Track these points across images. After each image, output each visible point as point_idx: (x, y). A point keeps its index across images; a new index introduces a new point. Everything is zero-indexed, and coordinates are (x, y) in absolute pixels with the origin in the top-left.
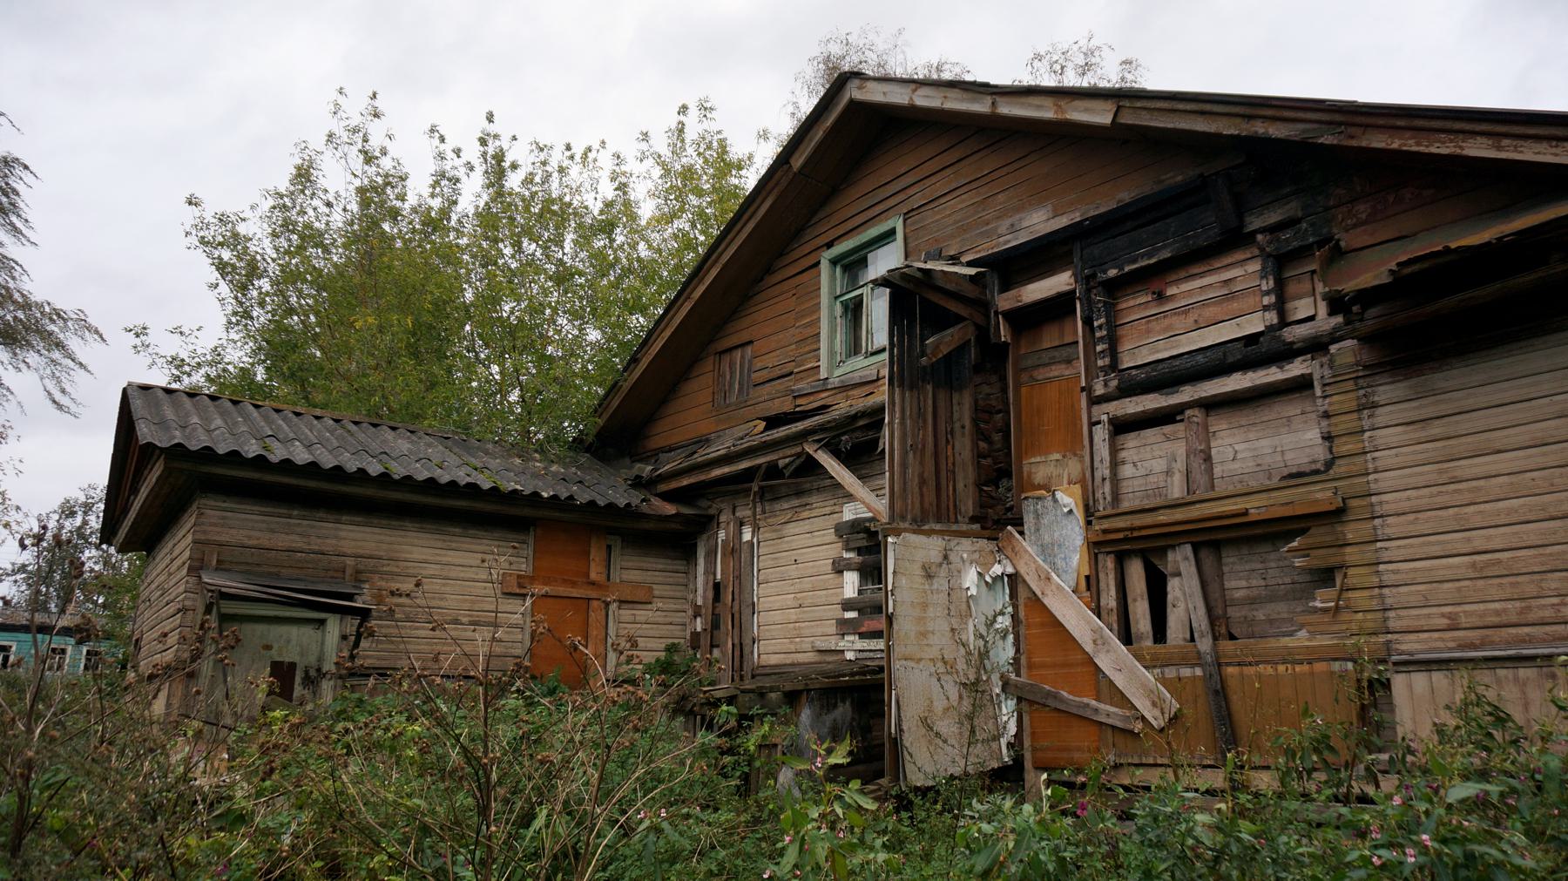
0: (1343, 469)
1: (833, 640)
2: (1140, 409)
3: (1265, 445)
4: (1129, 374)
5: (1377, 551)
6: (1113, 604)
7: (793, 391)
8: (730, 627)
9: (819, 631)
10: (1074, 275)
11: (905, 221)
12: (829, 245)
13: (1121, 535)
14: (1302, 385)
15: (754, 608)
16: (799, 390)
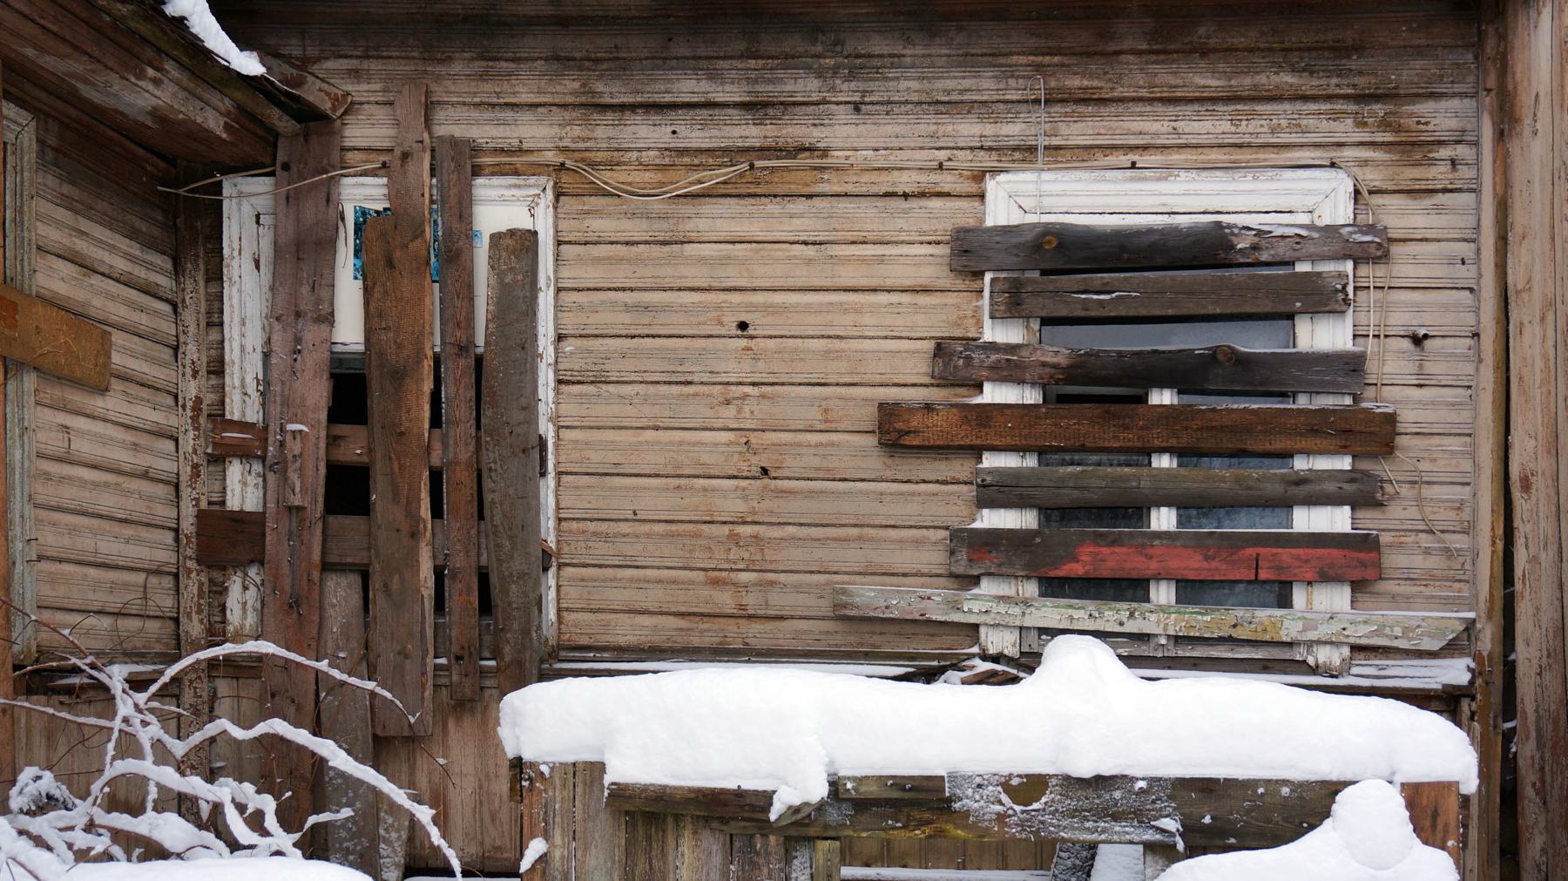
8: (425, 511)
9: (854, 557)
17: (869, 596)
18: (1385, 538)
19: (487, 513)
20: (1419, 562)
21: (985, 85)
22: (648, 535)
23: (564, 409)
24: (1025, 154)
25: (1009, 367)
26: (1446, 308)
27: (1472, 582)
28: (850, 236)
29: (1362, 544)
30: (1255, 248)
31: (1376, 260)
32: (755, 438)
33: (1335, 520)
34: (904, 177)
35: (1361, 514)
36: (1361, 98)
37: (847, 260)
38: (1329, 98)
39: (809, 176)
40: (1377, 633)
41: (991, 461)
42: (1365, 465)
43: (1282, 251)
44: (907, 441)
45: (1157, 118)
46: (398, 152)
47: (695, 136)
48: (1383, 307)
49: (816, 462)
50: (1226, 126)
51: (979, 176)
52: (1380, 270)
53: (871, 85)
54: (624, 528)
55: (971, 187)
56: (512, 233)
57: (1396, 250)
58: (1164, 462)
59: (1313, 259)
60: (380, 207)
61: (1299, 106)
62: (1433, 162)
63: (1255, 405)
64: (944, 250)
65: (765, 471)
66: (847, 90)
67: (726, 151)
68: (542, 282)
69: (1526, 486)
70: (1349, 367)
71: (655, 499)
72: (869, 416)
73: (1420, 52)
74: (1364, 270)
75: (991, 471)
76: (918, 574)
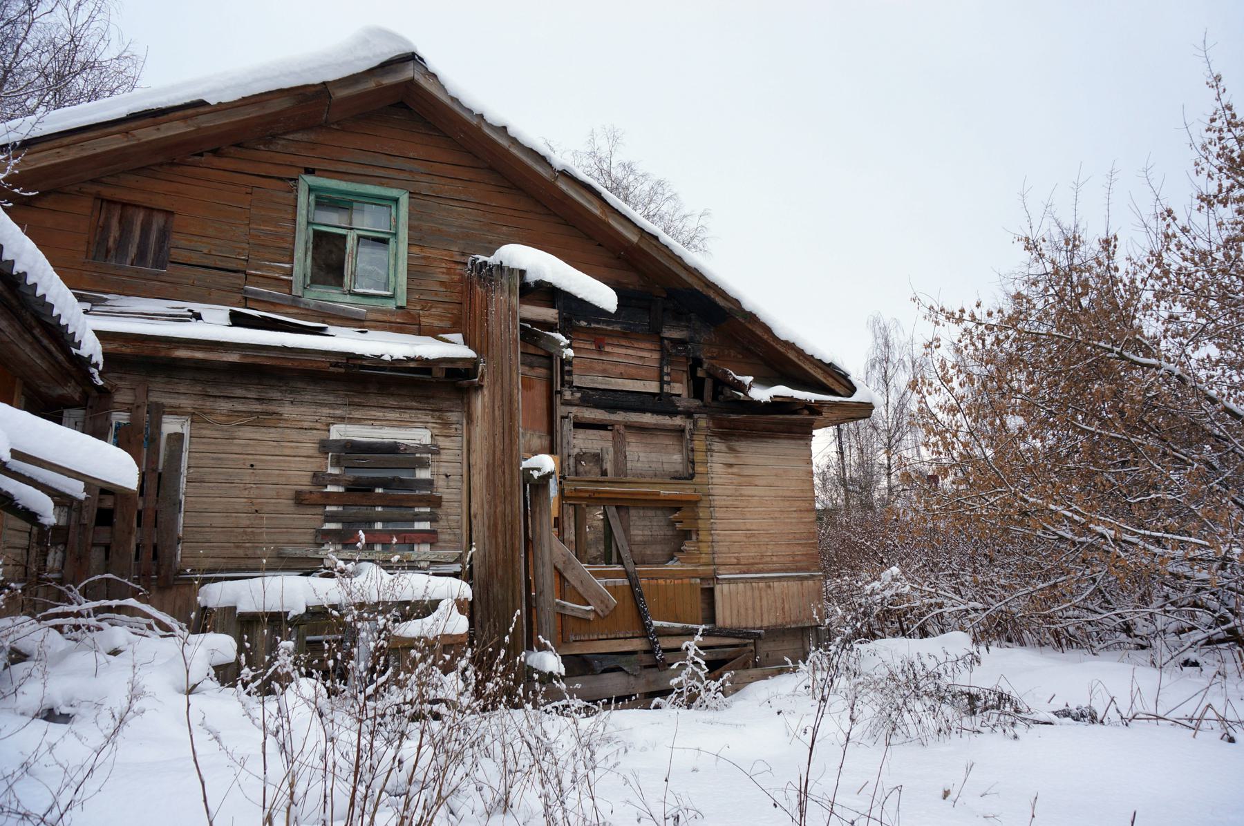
0: (699, 480)
1: (312, 550)
2: (592, 416)
3: (654, 457)
5: (712, 523)
6: (573, 538)
9: (284, 538)
10: (559, 313)
13: (587, 495)
14: (680, 431)
15: (180, 507)
17: (290, 550)
18: (439, 530)
19: (158, 526)
20: (447, 537)
21: (331, 399)
24: (342, 419)
25: (335, 480)
26: (454, 467)
27: (461, 542)
28: (288, 440)
29: (433, 532)
30: (405, 449)
31: (437, 454)
32: (254, 500)
33: (426, 526)
34: (306, 423)
35: (433, 524)
36: (433, 410)
37: (286, 447)
38: (425, 410)
39: (276, 421)
41: (329, 509)
42: (434, 510)
43: (413, 451)
44: (304, 502)
45: (380, 412)
46: (135, 405)
47: (240, 407)
48: (439, 467)
49: (273, 508)
51: (328, 425)
52: (438, 457)
53: (298, 396)
54: (207, 529)
55: (326, 428)
56: (176, 434)
57: (442, 451)
58: (379, 509)
59: (421, 453)
60: (125, 422)
61: (417, 411)
62: (451, 429)
63: (405, 493)
64: (317, 445)
65: (257, 511)
66: (289, 397)
67: (249, 412)
68: (184, 450)
69: (475, 517)
70: (429, 483)
71: (218, 520)
72: (291, 494)
73: (448, 400)
74: (433, 457)
75: (328, 511)
76: (305, 543)
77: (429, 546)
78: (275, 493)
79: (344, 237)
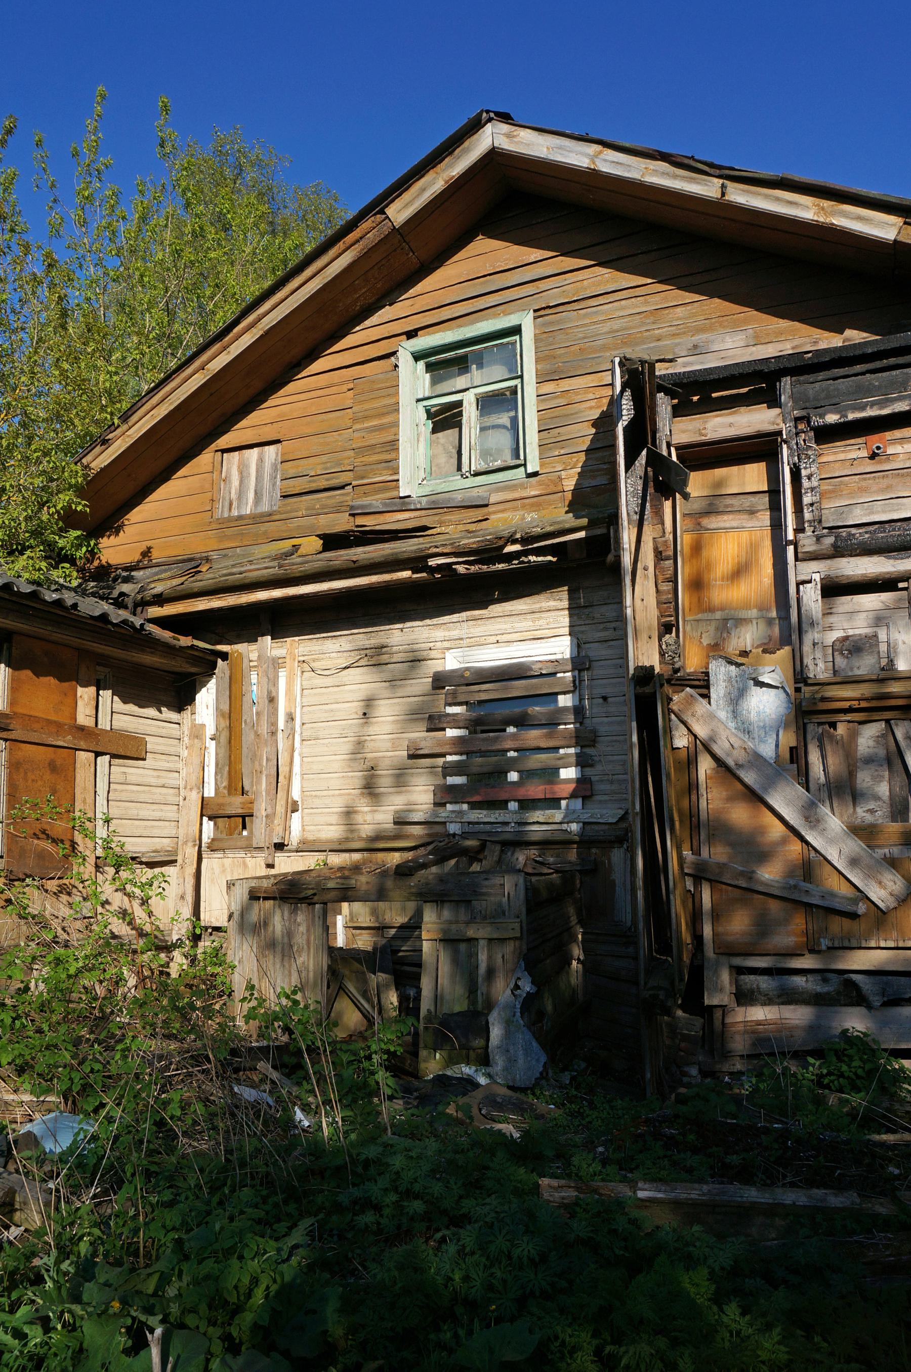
4: (849, 534)
7: (352, 508)
11: (535, 318)
12: (411, 334)
16: (362, 507)
22: (333, 796)
23: (305, 750)
40: (591, 817)
42: (585, 750)
50: (531, 623)
57: (594, 664)
65: (372, 768)
77: (580, 800)
78: (389, 745)
79: (459, 404)
